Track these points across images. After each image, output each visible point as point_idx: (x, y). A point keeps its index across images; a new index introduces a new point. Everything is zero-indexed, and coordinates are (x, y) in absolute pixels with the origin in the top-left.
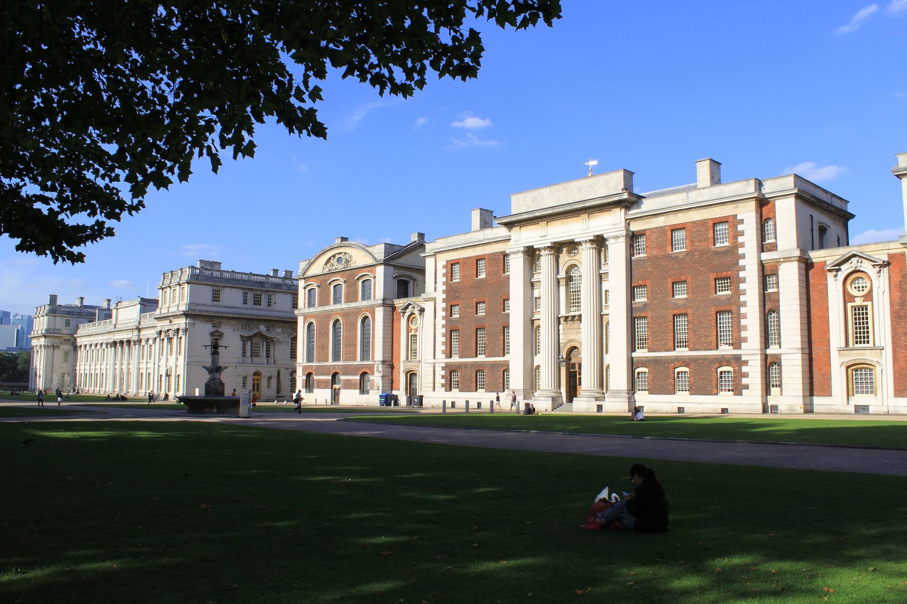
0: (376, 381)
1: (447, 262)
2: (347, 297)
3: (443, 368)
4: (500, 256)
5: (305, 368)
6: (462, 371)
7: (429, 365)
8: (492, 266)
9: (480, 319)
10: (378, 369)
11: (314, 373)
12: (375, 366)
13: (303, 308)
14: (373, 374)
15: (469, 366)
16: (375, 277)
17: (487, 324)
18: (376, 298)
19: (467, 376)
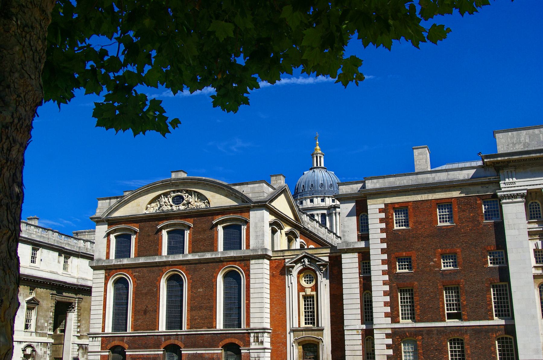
0: (252, 355)
1: (386, 205)
2: (193, 246)
3: (388, 336)
4: (476, 200)
5: (106, 341)
6: (423, 338)
7: (355, 332)
8: (463, 211)
9: (450, 273)
10: (258, 339)
11: (126, 346)
12: (252, 335)
13: (105, 258)
14: (248, 344)
15: (435, 332)
16: (247, 222)
17: (462, 280)
18: (251, 248)
19: (432, 345)
